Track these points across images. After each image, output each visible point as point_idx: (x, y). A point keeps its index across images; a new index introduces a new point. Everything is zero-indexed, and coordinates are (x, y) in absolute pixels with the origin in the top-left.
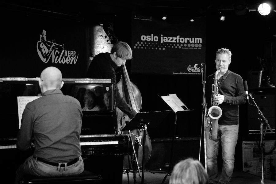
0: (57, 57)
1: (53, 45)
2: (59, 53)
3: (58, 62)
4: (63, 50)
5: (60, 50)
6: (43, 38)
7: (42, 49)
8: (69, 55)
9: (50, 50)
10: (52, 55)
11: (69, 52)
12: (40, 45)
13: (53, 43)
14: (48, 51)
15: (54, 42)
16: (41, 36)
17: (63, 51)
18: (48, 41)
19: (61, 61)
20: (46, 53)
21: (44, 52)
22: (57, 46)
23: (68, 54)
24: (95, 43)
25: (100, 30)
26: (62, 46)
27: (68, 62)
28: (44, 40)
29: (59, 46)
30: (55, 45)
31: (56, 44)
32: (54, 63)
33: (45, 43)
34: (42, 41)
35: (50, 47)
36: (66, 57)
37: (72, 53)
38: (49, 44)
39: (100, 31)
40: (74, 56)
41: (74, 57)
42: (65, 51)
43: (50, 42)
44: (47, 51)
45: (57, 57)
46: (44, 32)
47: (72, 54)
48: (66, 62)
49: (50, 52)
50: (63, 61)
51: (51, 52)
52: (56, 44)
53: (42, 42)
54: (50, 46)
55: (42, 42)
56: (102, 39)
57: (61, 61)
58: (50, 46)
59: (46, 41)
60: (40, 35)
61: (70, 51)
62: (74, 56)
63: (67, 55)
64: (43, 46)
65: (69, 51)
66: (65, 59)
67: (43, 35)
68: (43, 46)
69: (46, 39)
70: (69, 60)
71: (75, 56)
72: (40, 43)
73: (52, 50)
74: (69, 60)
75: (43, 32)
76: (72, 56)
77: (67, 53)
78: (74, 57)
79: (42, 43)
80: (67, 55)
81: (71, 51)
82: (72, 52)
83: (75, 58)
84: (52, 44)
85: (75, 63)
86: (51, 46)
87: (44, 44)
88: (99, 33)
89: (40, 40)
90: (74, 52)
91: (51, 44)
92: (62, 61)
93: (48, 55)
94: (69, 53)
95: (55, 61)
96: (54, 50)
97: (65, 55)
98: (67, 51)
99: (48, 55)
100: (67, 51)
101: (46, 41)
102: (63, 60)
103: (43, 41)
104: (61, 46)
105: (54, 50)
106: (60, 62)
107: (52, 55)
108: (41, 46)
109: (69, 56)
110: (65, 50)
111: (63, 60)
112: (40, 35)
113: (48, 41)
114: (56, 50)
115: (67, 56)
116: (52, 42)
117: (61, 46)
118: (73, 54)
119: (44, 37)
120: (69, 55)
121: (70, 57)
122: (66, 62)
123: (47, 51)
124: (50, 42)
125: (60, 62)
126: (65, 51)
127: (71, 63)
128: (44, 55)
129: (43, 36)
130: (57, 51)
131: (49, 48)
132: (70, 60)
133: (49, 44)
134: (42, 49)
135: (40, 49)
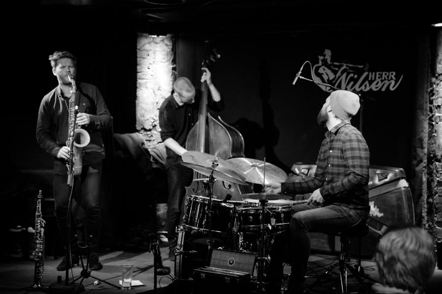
0: (352, 83)
1: (342, 68)
2: (356, 76)
5: (360, 73)
6: (324, 61)
7: (323, 74)
8: (379, 78)
9: (338, 74)
10: (341, 80)
11: (379, 74)
12: (318, 70)
13: (345, 65)
14: (334, 76)
15: (345, 63)
16: (321, 58)
17: (366, 74)
18: (335, 63)
19: (360, 87)
20: (331, 79)
22: (351, 68)
24: (438, 55)
26: (364, 67)
27: (376, 88)
28: (327, 63)
29: (358, 67)
30: (346, 66)
31: (351, 65)
33: (329, 67)
34: (322, 64)
35: (337, 71)
36: (371, 83)
38: (336, 66)
40: (390, 78)
42: (370, 73)
43: (338, 64)
44: (332, 76)
45: (352, 83)
46: (328, 53)
47: (386, 76)
48: (371, 89)
49: (337, 76)
50: (364, 88)
51: (339, 77)
52: (351, 65)
53: (323, 65)
54: (337, 69)
55: (323, 65)
57: (360, 87)
58: (337, 69)
59: (329, 62)
60: (319, 57)
61: (381, 73)
62: (390, 78)
63: (373, 79)
65: (378, 73)
66: (370, 85)
67: (324, 56)
68: (324, 69)
69: (331, 61)
70: (377, 86)
71: (392, 79)
72: (319, 67)
73: (342, 73)
74: (377, 86)
75: (324, 51)
76: (385, 79)
78: (389, 81)
79: (324, 67)
80: (373, 79)
81: (384, 73)
82: (387, 73)
83: (393, 82)
84: (343, 66)
85: (392, 89)
86: (340, 69)
87: (326, 68)
89: (318, 63)
90: (391, 73)
91: (339, 67)
92: (363, 87)
93: (334, 82)
94: (377, 76)
96: (345, 74)
97: (370, 79)
98: (374, 73)
99: (334, 82)
100: (374, 73)
101: (329, 62)
102: (366, 86)
103: (325, 63)
104: (362, 66)
105: (345, 74)
107: (341, 80)
108: (321, 71)
109: (378, 80)
110: (369, 71)
111: (366, 86)
112: (319, 57)
113: (335, 63)
115: (375, 80)
116: (343, 64)
117: (362, 66)
118: (388, 77)
119: (327, 59)
120: (379, 78)
122: (371, 89)
123: (332, 76)
124: (338, 64)
126: (370, 73)
127: (383, 89)
128: (326, 81)
129: (325, 58)
130: (352, 75)
131: (335, 72)
132: (380, 85)
133: (336, 66)
134: (323, 74)
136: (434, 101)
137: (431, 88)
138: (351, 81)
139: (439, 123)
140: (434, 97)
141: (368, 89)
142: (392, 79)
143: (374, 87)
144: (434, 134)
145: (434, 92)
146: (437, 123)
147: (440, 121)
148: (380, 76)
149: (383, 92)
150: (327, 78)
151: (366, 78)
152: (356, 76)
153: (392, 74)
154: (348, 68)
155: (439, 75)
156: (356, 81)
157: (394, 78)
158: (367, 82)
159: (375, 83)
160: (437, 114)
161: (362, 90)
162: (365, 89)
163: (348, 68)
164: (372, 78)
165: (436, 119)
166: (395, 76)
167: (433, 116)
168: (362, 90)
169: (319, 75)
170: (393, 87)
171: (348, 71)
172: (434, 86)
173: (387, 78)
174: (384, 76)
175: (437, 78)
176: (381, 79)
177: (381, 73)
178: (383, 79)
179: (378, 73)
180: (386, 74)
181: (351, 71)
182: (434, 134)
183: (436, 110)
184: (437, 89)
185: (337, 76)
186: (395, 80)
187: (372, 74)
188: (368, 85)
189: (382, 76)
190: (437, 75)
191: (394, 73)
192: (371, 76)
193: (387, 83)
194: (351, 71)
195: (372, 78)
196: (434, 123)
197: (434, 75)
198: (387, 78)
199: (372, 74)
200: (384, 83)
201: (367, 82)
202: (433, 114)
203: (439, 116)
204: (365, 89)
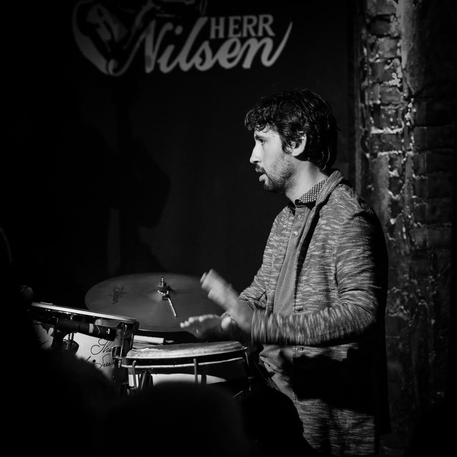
0: (170, 49)
1: (145, 9)
2: (179, 30)
3: (178, 66)
4: (197, 16)
7: (97, 26)
8: (236, 32)
11: (236, 22)
17: (201, 23)
21: (105, 36)
23: (231, 34)
27: (230, 60)
32: (153, 72)
36: (216, 46)
37: (250, 22)
40: (260, 34)
41: (259, 39)
42: (213, 20)
45: (170, 49)
47: (250, 27)
48: (217, 64)
49: (134, 31)
61: (239, 18)
63: (221, 35)
65: (232, 19)
66: (215, 51)
71: (266, 34)
77: (221, 28)
78: (259, 39)
80: (221, 35)
81: (246, 18)
82: (254, 18)
83: (269, 43)
85: (267, 63)
90: (262, 17)
92: (197, 60)
93: (125, 47)
94: (232, 27)
95: (157, 66)
96: (153, 25)
97: (213, 36)
98: (222, 20)
99: (125, 47)
100: (222, 20)
102: (203, 56)
105: (153, 25)
106: (185, 67)
109: (234, 38)
110: (209, 14)
111: (203, 56)
114: (165, 21)
115: (226, 38)
118: (256, 29)
120: (236, 32)
121: (243, 40)
122: (217, 64)
125: (185, 67)
126: (213, 20)
127: (247, 64)
130: (168, 27)
131: (127, 21)
132: (238, 52)
134: (97, 26)
135: (90, 31)
138: (170, 43)
139: (380, 154)
140: (365, 83)
141: (209, 64)
142: (266, 34)
143: (223, 58)
146: (374, 155)
147: (382, 151)
148: (237, 27)
149: (247, 70)
151: (204, 35)
152: (179, 30)
153: (266, 21)
154: (158, 8)
156: (179, 43)
157: (271, 33)
158: (206, 46)
159: (227, 45)
160: (375, 131)
161: (194, 67)
162: (201, 64)
163: (158, 8)
164: (217, 32)
166: (272, 26)
167: (367, 133)
168: (194, 67)
169: (90, 31)
170: (269, 58)
171: (159, 15)
172: (365, 50)
173: (253, 34)
174: (245, 26)
175: (369, 28)
176: (239, 35)
177: (239, 18)
178: (245, 35)
179: (232, 19)
180: (250, 22)
181: (167, 16)
184: (371, 60)
185: (134, 31)
186: (272, 37)
187: (217, 24)
188: (209, 53)
189: (240, 23)
191: (271, 19)
192: (217, 28)
193: (254, 46)
194: (167, 16)
195: (217, 32)
198: (253, 34)
199: (217, 24)
200: (248, 47)
201: (206, 46)
203: (379, 136)
204: (201, 64)
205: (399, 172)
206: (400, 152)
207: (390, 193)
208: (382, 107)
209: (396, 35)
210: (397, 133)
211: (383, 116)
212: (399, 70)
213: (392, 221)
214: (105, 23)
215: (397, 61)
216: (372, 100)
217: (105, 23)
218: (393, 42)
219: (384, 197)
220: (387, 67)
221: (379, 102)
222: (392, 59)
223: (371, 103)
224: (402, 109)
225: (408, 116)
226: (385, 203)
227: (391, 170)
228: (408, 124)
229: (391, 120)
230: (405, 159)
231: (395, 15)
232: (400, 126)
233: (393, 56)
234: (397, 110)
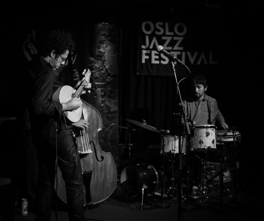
21: (32, 53)
25: (102, 29)
39: (102, 30)
56: (104, 38)
64: (31, 46)
68: (31, 46)
88: (101, 32)
135: (28, 50)
136: (94, 74)
137: (90, 65)
139: (98, 89)
144: (95, 97)
145: (94, 68)
150: (34, 53)
155: (97, 56)
165: (96, 86)
169: (28, 50)
175: (95, 58)
182: (95, 97)
183: (95, 80)
190: (96, 56)
196: (94, 89)
197: (93, 56)
202: (93, 83)
205: (104, 93)
206: (104, 88)
207: (101, 98)
208: (99, 78)
209: (104, 60)
210: (104, 84)
211: (99, 80)
212: (104, 69)
213: (102, 105)
214: (33, 49)
215: (104, 67)
216: (96, 76)
217: (33, 49)
218: (102, 62)
219: (100, 100)
220: (101, 68)
221: (98, 76)
222: (102, 66)
223: (95, 76)
224: (105, 78)
225: (107, 80)
226: (100, 101)
227: (102, 93)
228: (107, 82)
229: (102, 81)
230: (106, 90)
231: (104, 55)
232: (104, 82)
233: (102, 65)
234: (103, 79)
